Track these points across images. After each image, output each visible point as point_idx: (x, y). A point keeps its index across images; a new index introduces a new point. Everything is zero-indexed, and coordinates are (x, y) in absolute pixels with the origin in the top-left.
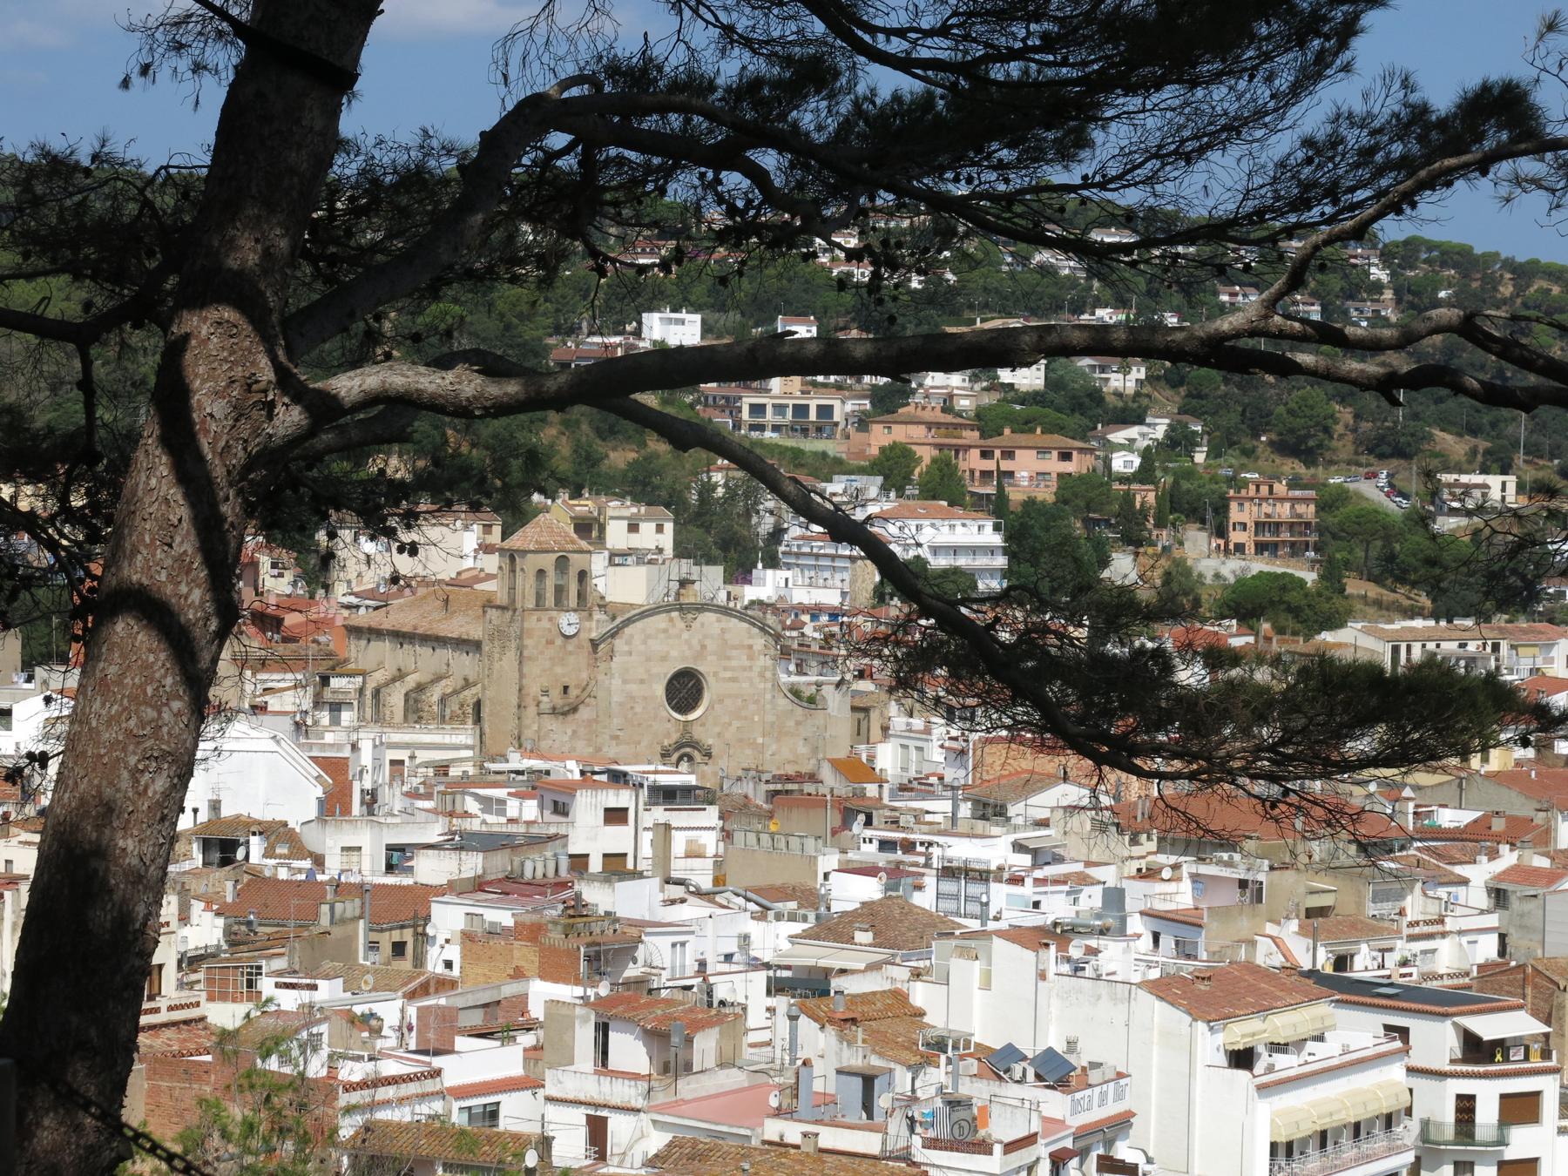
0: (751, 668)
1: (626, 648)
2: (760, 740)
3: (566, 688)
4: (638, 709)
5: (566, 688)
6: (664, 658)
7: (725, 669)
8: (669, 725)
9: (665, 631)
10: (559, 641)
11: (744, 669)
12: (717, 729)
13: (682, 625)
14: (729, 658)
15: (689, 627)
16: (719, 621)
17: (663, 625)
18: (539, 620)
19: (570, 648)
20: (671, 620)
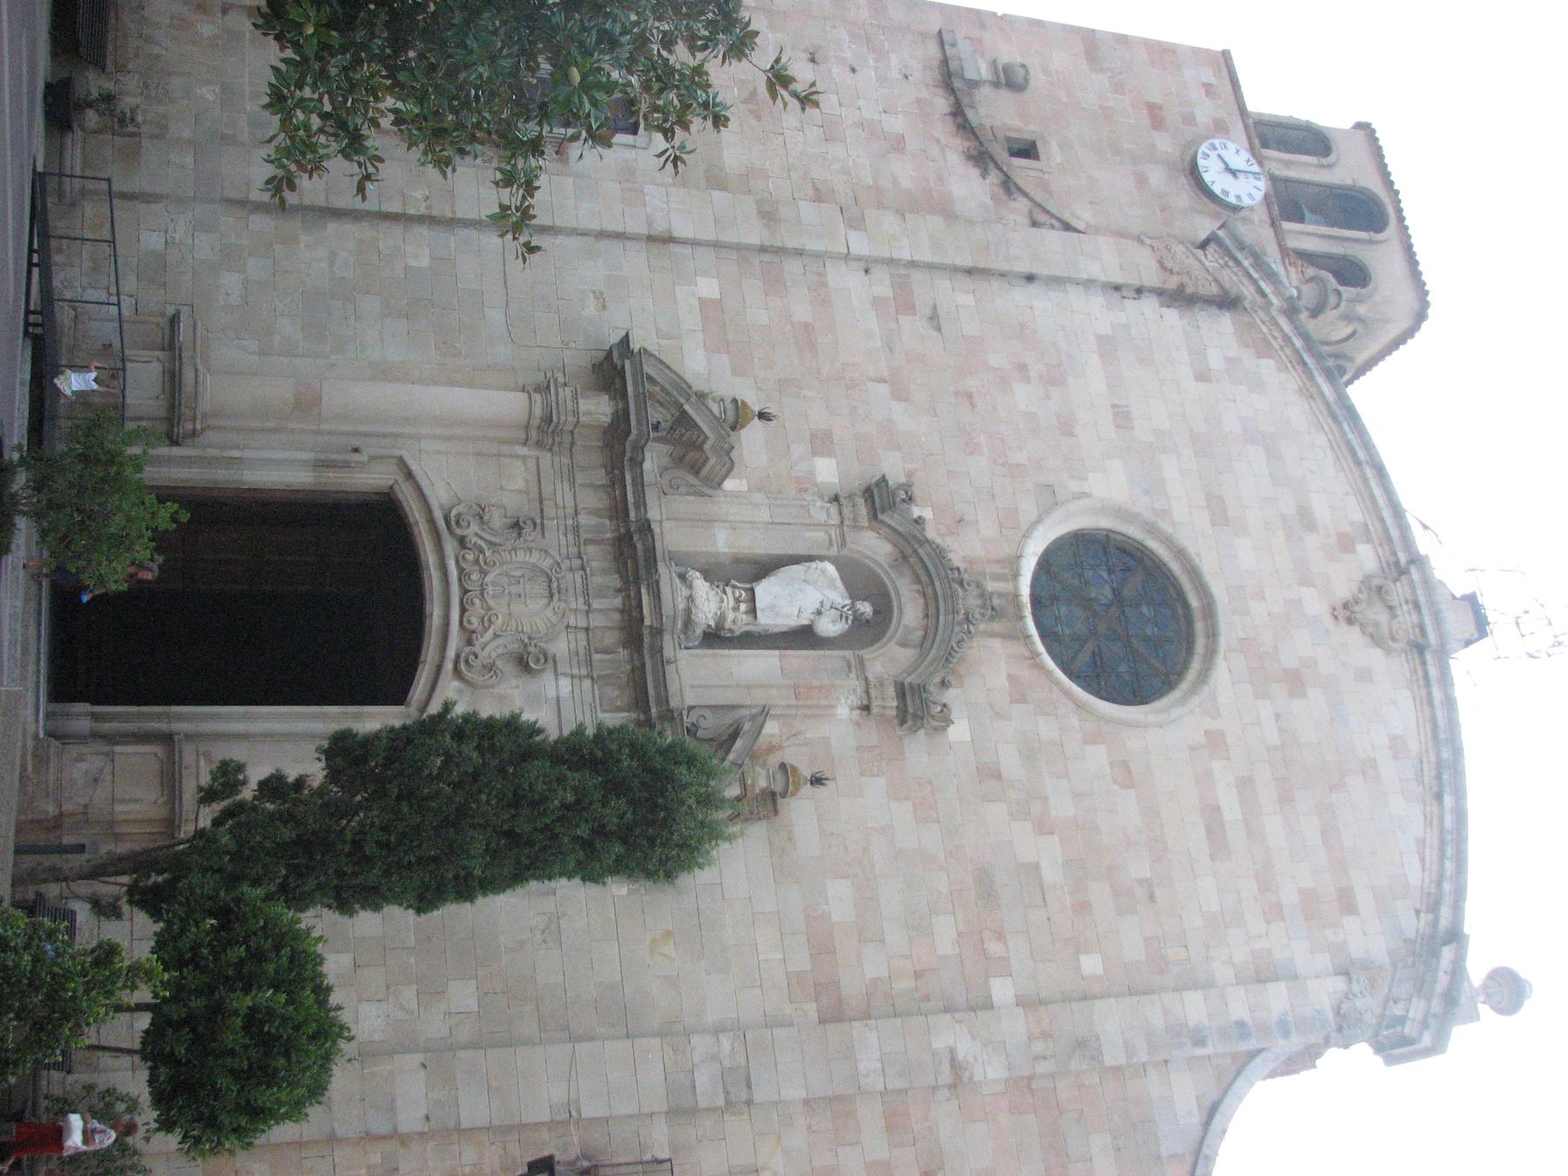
0: (1275, 912)
1: (1215, 361)
2: (1002, 991)
3: (1027, 151)
4: (1024, 396)
5: (1027, 151)
6: (1218, 511)
7: (1245, 784)
8: (988, 528)
9: (1306, 519)
10: (1165, 144)
11: (1266, 885)
12: (1011, 764)
13: (1344, 589)
14: (1285, 799)
15: (1347, 612)
16: (1397, 746)
17: (1321, 509)
18: (1208, 88)
19: (1157, 177)
20: (1346, 544)
